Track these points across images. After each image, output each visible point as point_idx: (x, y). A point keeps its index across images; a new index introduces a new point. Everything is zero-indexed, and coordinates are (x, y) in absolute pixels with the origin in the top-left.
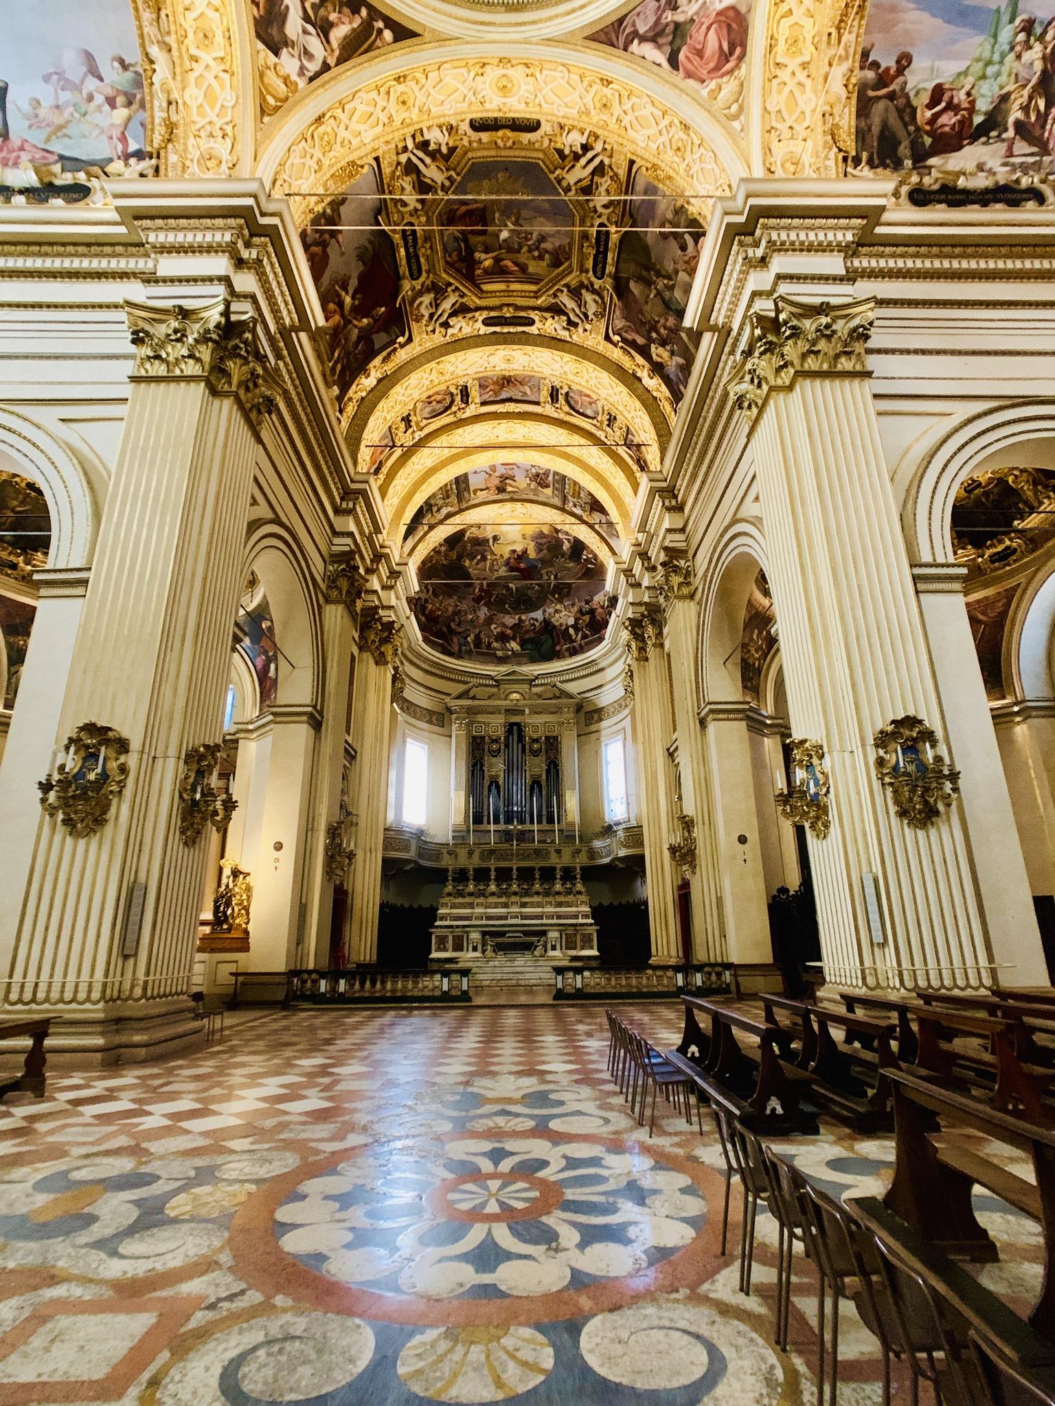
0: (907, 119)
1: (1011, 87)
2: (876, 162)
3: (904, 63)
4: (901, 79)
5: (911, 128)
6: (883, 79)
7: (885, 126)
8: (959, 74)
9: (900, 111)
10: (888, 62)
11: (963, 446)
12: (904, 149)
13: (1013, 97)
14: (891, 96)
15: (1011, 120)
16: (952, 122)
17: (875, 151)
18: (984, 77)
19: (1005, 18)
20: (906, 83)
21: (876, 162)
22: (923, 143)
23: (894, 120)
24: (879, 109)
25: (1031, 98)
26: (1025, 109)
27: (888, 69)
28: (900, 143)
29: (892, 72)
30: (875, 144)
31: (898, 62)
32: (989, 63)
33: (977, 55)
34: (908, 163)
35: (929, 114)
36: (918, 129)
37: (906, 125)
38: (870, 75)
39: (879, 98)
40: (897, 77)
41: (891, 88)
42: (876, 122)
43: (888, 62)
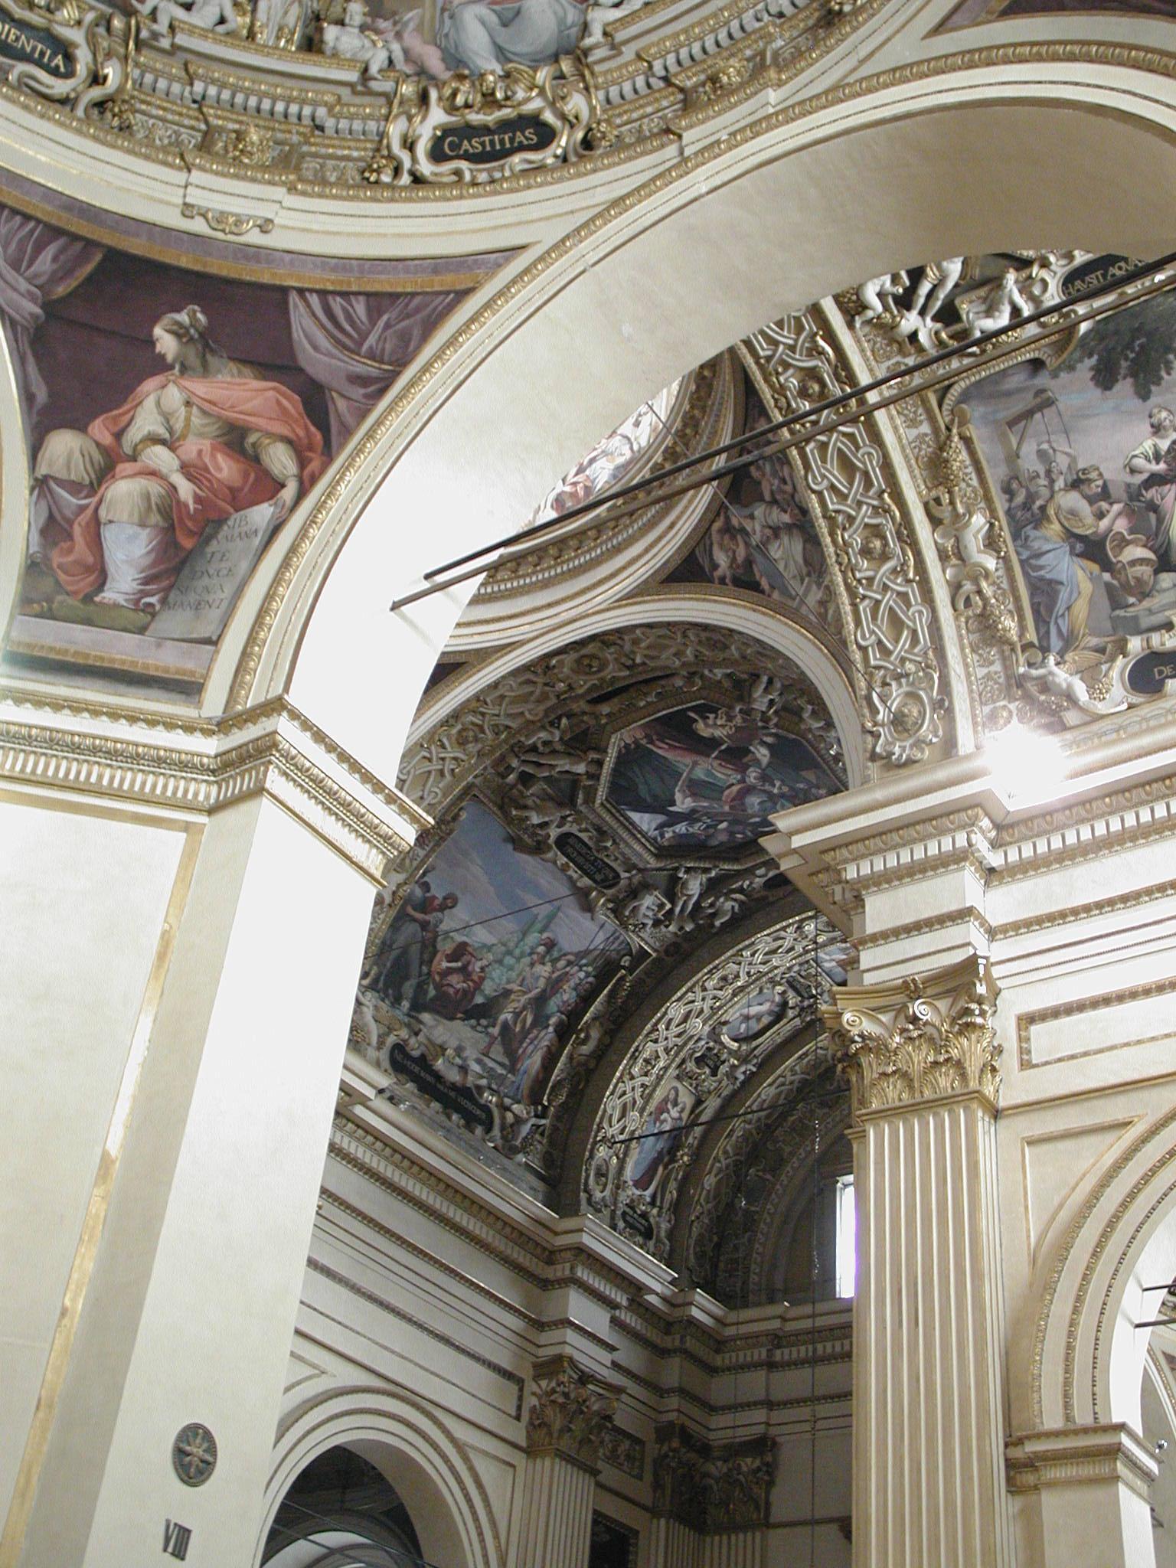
0: (426, 957)
1: (515, 987)
2: (381, 985)
3: (449, 902)
4: (439, 914)
5: (425, 969)
6: (425, 906)
7: (405, 950)
8: (484, 946)
9: (424, 946)
10: (438, 893)
11: (313, 1429)
12: (408, 988)
13: (513, 997)
14: (424, 926)
15: (502, 1017)
16: (458, 986)
17: (385, 972)
18: (500, 962)
19: (538, 926)
20: (441, 921)
21: (381, 985)
22: (426, 992)
23: (415, 949)
24: (410, 929)
25: (524, 1008)
26: (517, 1015)
27: (434, 897)
28: (407, 978)
29: (437, 902)
30: (389, 965)
31: (445, 898)
32: (509, 953)
33: (504, 940)
34: (406, 1004)
35: (445, 964)
36: (429, 974)
37: (421, 964)
38: (418, 892)
39: (415, 920)
40: (435, 910)
41: (427, 917)
42: (401, 940)
43: (438, 893)
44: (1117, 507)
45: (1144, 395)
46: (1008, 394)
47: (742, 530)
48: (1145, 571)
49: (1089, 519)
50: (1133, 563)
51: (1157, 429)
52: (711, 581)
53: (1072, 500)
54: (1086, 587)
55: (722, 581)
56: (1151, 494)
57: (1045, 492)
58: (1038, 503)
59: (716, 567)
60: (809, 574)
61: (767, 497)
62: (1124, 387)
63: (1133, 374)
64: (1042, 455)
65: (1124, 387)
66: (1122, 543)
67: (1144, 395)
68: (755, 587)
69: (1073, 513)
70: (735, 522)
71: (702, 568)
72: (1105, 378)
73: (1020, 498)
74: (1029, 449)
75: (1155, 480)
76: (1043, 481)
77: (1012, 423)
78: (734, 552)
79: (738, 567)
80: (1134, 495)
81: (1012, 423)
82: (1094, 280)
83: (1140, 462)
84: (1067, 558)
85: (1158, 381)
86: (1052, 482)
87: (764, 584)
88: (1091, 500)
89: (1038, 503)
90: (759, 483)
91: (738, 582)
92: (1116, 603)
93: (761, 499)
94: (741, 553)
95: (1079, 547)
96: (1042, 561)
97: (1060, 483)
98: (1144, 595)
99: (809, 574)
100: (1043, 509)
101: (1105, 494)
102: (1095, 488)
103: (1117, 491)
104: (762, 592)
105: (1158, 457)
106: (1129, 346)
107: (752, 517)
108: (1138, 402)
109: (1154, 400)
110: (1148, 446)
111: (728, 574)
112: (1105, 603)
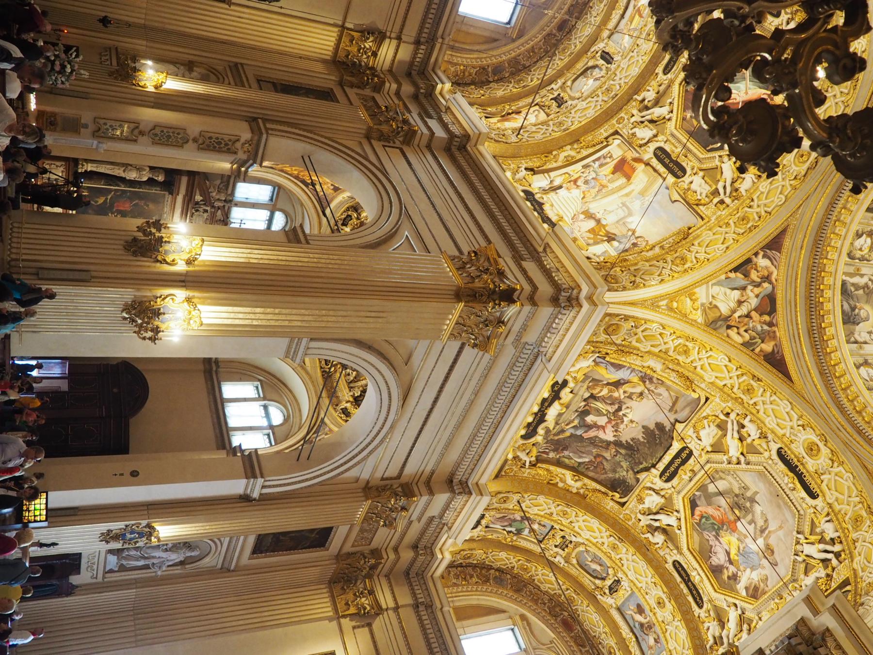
44: (622, 397)
45: (643, 427)
46: (685, 407)
47: (758, 285)
48: (595, 392)
49: (627, 389)
50: (601, 390)
51: (632, 421)
52: (762, 249)
53: (639, 389)
54: (607, 376)
55: (756, 254)
56: (616, 406)
57: (648, 386)
58: (648, 382)
59: (764, 256)
60: (711, 303)
61: (753, 314)
62: (652, 426)
63: (653, 431)
64: (660, 395)
65: (652, 426)
66: (610, 391)
67: (643, 427)
68: (735, 270)
69: (634, 387)
70: (766, 285)
71: (770, 250)
72: (660, 426)
73: (655, 380)
74: (665, 394)
75: (620, 409)
76: (652, 388)
77: (677, 398)
78: (758, 272)
79: (752, 268)
80: (621, 403)
81: (677, 398)
82: (684, 455)
83: (628, 411)
84: (623, 377)
85: (643, 433)
86: (649, 390)
87: (732, 275)
88: (632, 394)
89: (648, 382)
90: (760, 315)
91: (748, 261)
92: (593, 380)
93: (755, 310)
94: (754, 275)
95: (622, 382)
96: (629, 371)
97: (646, 391)
98: (588, 388)
99: (711, 303)
100: (644, 382)
101: (630, 397)
102: (634, 397)
103: (627, 400)
104: (731, 271)
105: (624, 415)
106: (660, 438)
107: (757, 296)
108: (645, 424)
109: (640, 427)
110: (630, 416)
111: (754, 259)
112: (597, 377)
